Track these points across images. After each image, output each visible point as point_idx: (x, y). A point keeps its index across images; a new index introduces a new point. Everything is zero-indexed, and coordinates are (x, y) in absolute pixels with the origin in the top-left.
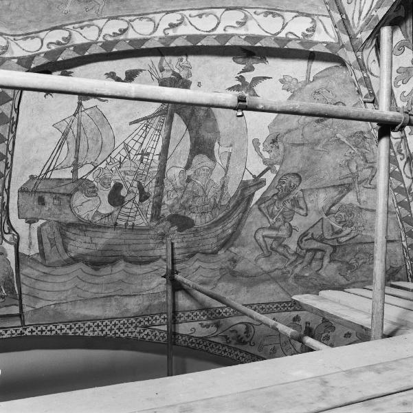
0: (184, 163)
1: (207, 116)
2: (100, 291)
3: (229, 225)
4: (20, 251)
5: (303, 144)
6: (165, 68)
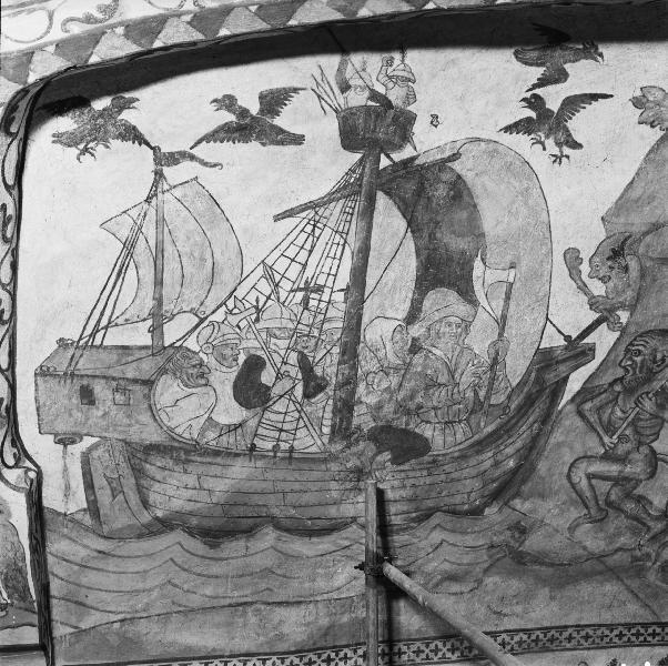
0: (402, 310)
1: (454, 198)
2: (221, 591)
3: (510, 450)
4: (46, 503)
6: (351, 83)
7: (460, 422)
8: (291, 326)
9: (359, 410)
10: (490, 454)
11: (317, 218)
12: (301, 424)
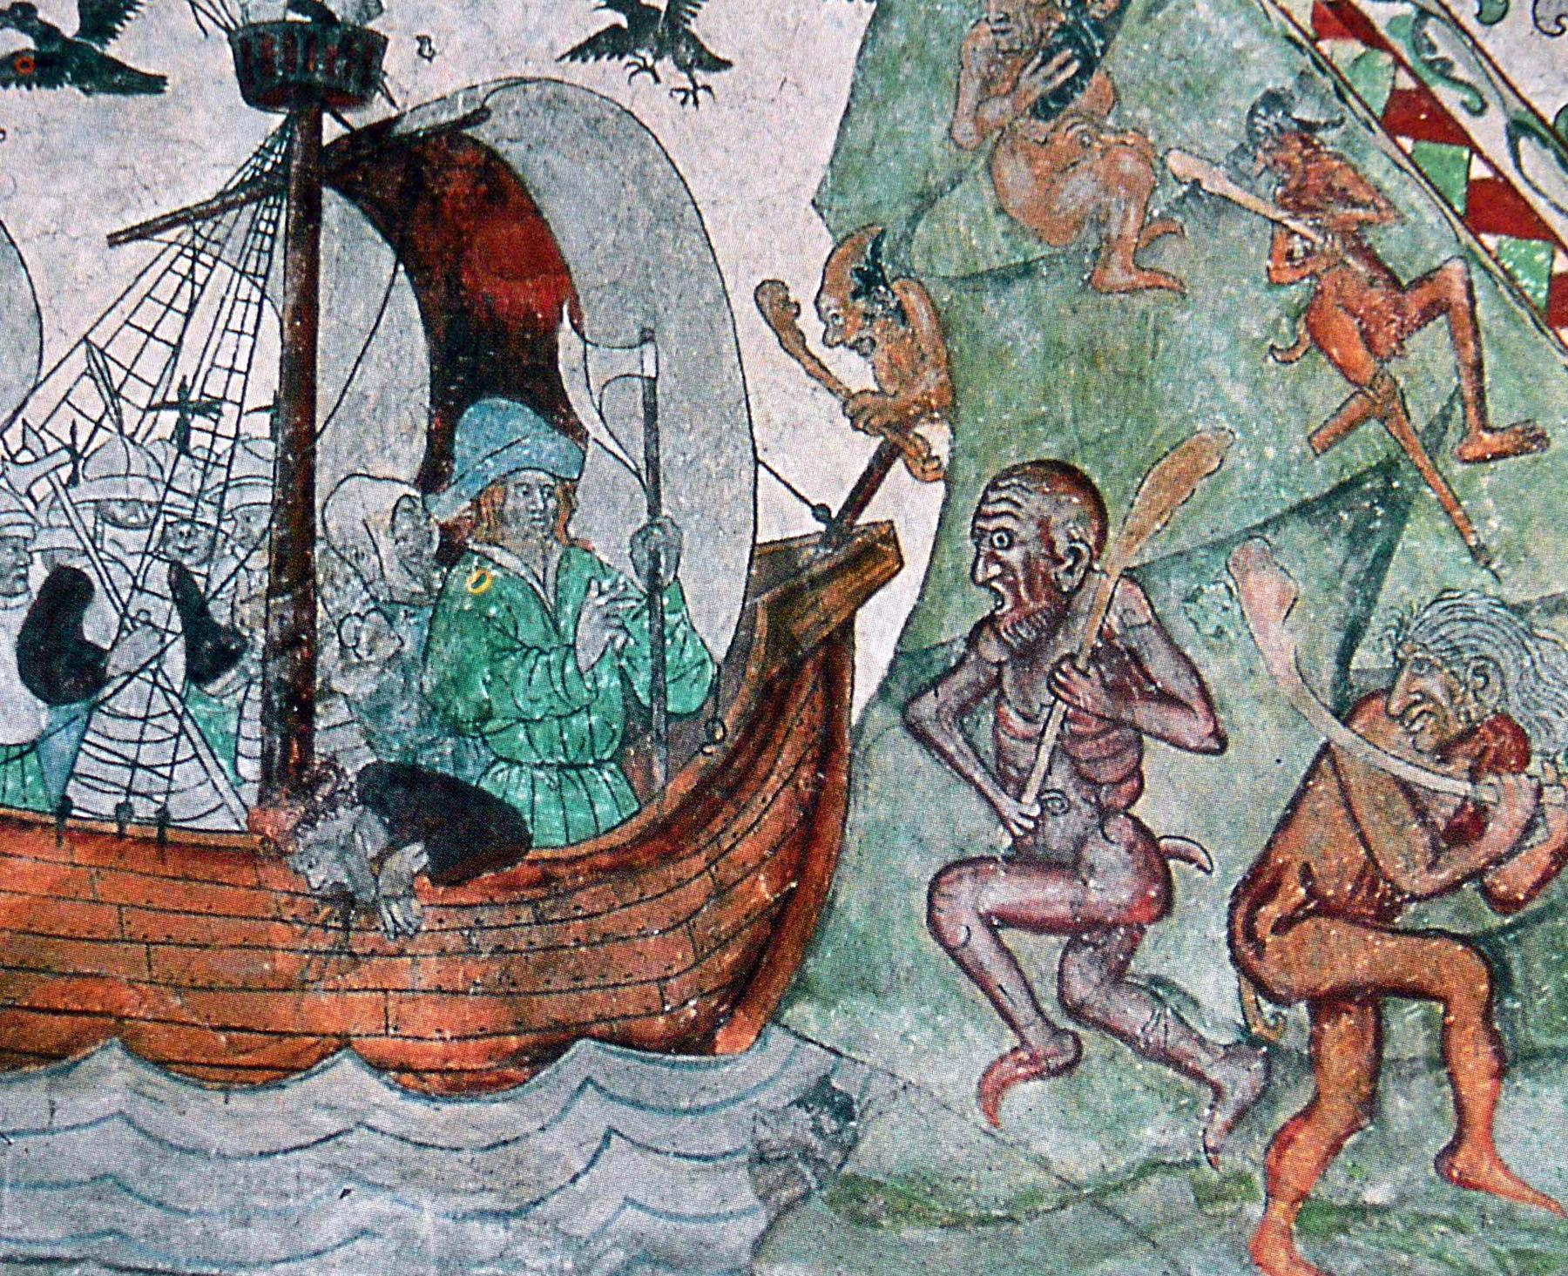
1: (489, 196)
5: (1028, 270)
7: (599, 765)
8: (149, 495)
9: (328, 715)
10: (698, 863)
11: (198, 243)
12: (186, 751)
